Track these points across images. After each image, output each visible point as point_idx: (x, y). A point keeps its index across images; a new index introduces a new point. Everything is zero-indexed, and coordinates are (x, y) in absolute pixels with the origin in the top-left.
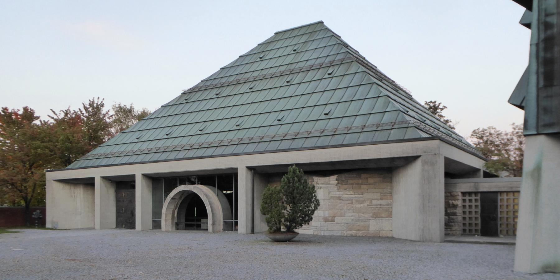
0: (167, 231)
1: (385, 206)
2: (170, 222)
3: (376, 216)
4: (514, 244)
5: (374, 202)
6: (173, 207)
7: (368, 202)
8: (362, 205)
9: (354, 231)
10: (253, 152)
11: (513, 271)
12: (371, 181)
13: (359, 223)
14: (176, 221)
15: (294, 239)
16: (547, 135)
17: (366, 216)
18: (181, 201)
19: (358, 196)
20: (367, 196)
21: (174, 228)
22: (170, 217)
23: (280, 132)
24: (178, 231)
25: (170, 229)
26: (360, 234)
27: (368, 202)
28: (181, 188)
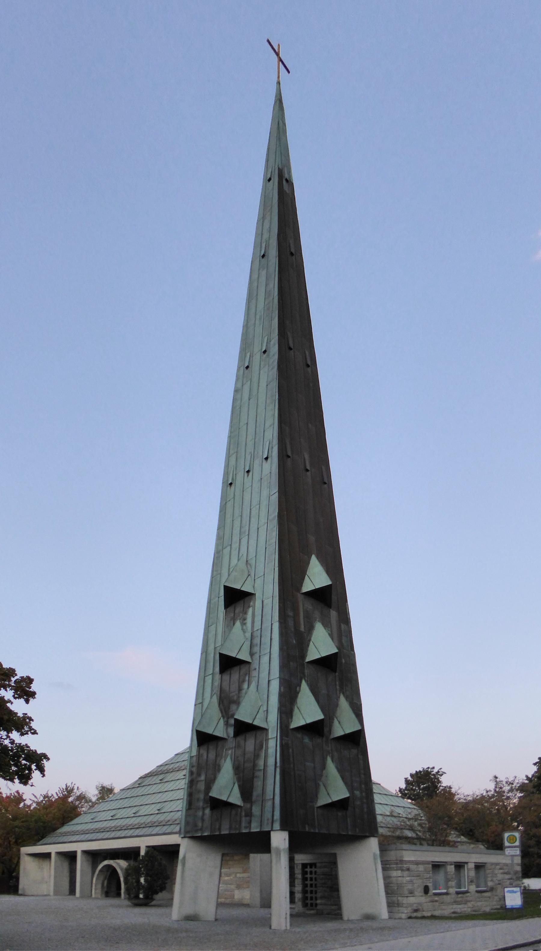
0: (96, 898)
1: (247, 879)
2: (99, 891)
3: (239, 887)
4: (219, 905)
5: (238, 875)
6: (102, 878)
7: (233, 876)
8: (229, 878)
9: (222, 899)
10: (156, 834)
11: (62, 909)
12: (236, 858)
13: (226, 893)
14: (105, 890)
15: (150, 904)
16: (190, 837)
17: (233, 887)
18: (109, 873)
19: (226, 870)
20: (232, 870)
21: (104, 895)
22: (100, 886)
23: (149, 820)
24: (107, 898)
25: (99, 896)
26: (228, 901)
27: (233, 876)
28: (106, 862)
